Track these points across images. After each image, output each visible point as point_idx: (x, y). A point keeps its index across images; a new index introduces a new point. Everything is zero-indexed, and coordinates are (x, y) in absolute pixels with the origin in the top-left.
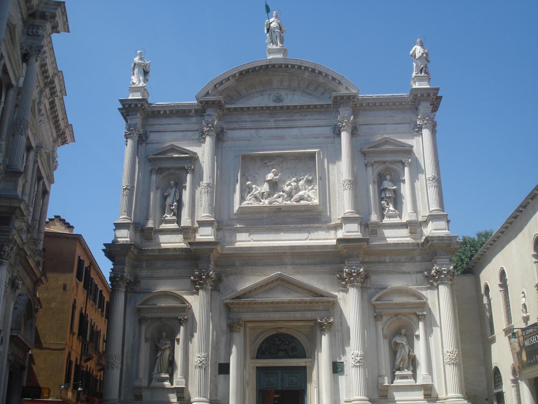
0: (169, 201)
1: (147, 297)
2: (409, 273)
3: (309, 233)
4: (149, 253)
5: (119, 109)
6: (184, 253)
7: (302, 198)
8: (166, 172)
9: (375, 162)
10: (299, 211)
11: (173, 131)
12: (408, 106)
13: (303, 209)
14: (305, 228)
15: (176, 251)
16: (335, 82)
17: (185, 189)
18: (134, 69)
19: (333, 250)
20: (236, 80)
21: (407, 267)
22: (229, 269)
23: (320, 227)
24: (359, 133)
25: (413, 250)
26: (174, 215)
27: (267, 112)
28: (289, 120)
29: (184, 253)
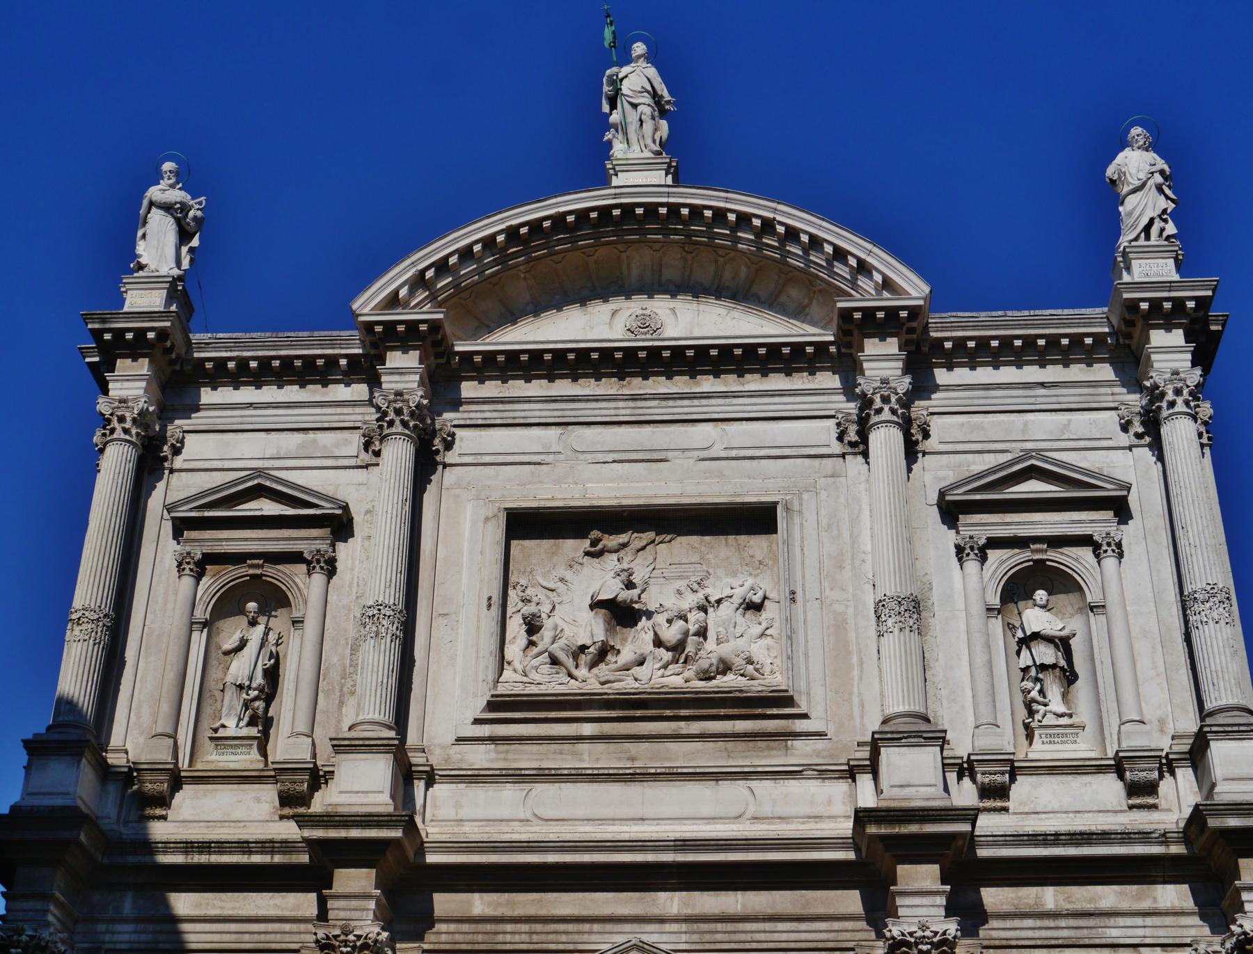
0: (240, 668)
7: (725, 667)
8: (233, 573)
9: (994, 543)
16: (846, 263)
24: (931, 444)
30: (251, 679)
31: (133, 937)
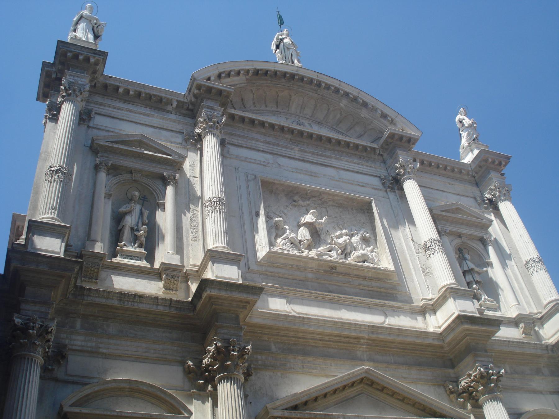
1: (87, 390)
2: (541, 392)
3: (386, 316)
4: (98, 300)
5: (45, 64)
6: (173, 311)
10: (364, 278)
11: (136, 123)
12: (466, 177)
13: (370, 274)
14: (376, 305)
15: (157, 305)
17: (163, 209)
18: (77, 23)
19: (436, 342)
20: (247, 79)
21: (537, 383)
22: (259, 357)
23: (399, 308)
25: (539, 356)
26: (140, 246)
27: (287, 136)
28: (321, 155)
29: (173, 311)
30: (137, 226)
31: (83, 344)
